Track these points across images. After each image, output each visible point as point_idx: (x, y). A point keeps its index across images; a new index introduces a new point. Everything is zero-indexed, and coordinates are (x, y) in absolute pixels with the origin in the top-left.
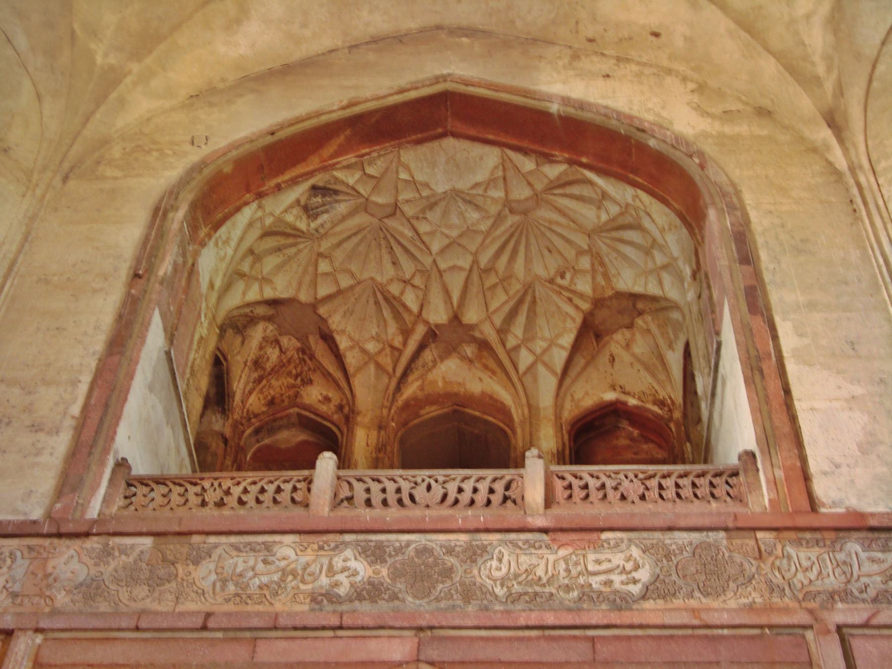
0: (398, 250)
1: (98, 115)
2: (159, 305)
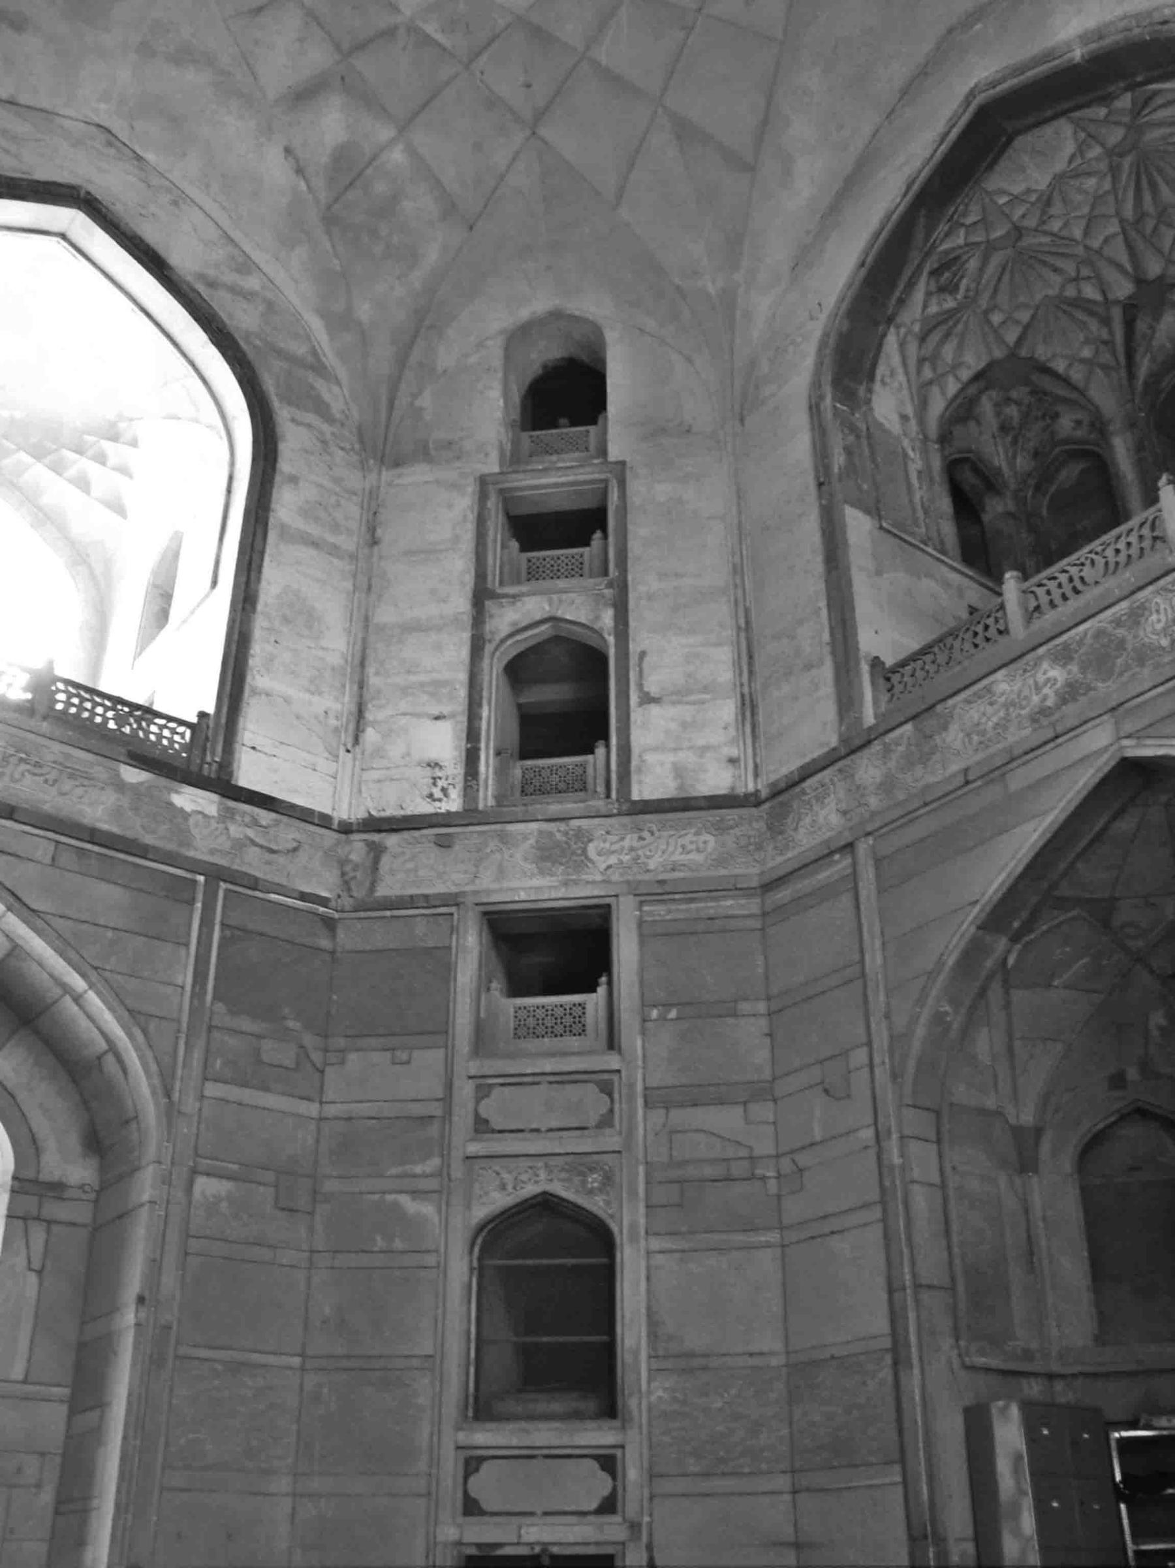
0: (1050, 259)
1: (738, 341)
2: (846, 502)
